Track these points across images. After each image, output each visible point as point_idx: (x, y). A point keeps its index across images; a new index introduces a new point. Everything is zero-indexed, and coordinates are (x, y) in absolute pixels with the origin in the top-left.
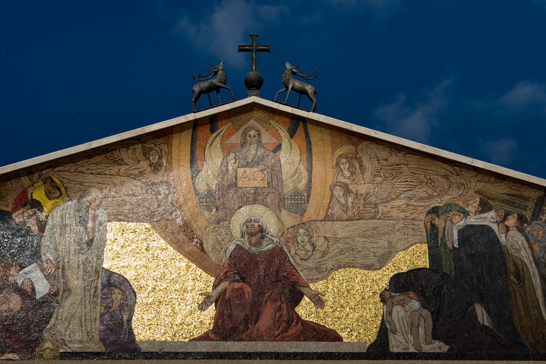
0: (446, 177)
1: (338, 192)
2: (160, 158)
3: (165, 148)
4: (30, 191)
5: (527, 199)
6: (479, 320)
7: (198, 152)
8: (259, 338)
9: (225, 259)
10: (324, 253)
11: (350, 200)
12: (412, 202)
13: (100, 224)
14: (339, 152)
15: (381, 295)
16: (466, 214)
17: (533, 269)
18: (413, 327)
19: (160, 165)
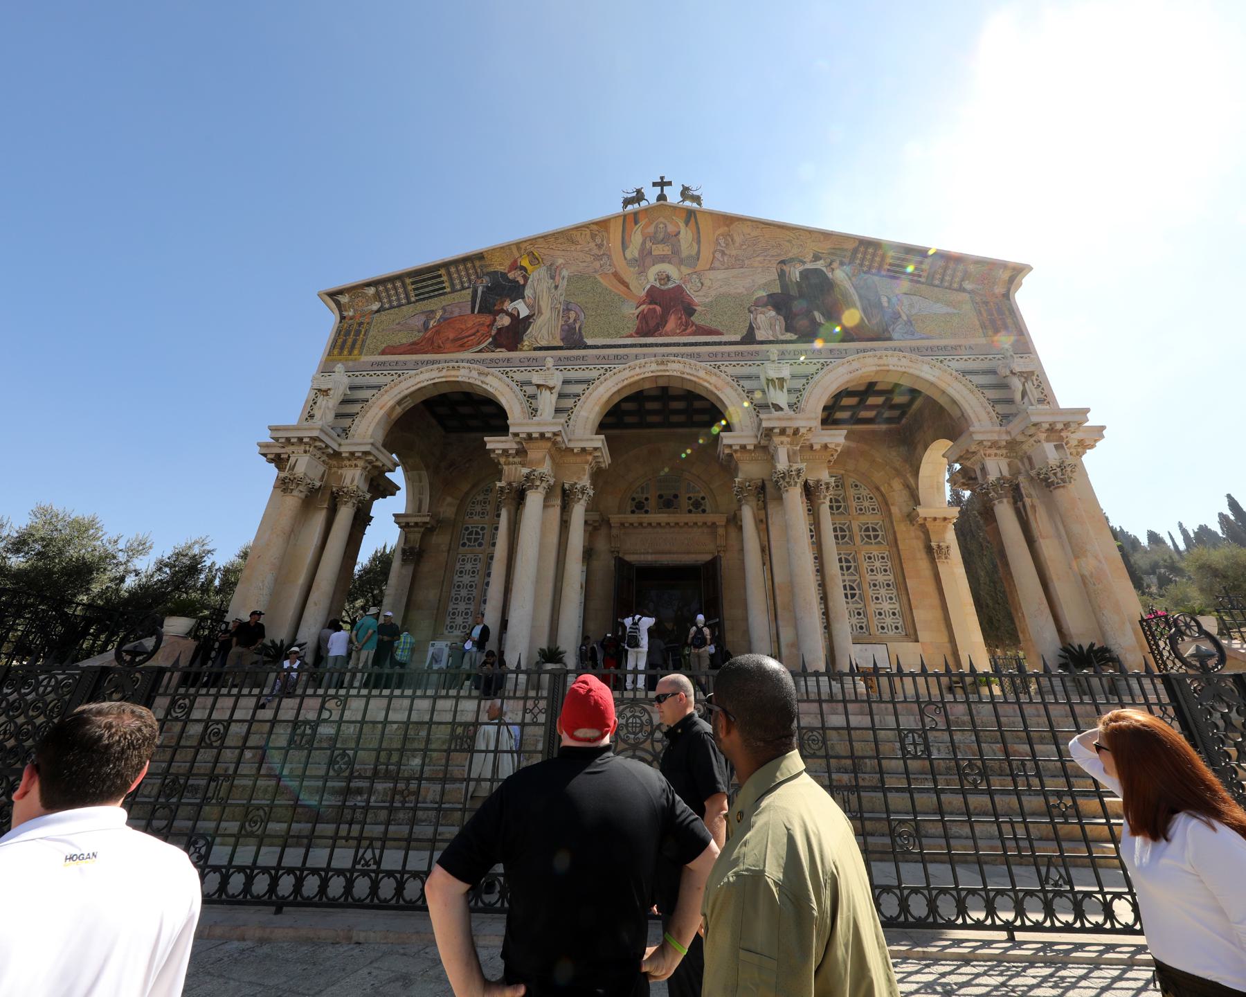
0: (789, 241)
1: (718, 255)
2: (602, 241)
3: (605, 234)
4: (519, 261)
5: (846, 250)
6: (818, 320)
7: (626, 238)
8: (667, 335)
9: (643, 293)
10: (710, 288)
11: (726, 259)
12: (768, 258)
13: (563, 278)
14: (718, 233)
15: (749, 309)
16: (804, 263)
17: (852, 291)
18: (772, 326)
19: (603, 245)
